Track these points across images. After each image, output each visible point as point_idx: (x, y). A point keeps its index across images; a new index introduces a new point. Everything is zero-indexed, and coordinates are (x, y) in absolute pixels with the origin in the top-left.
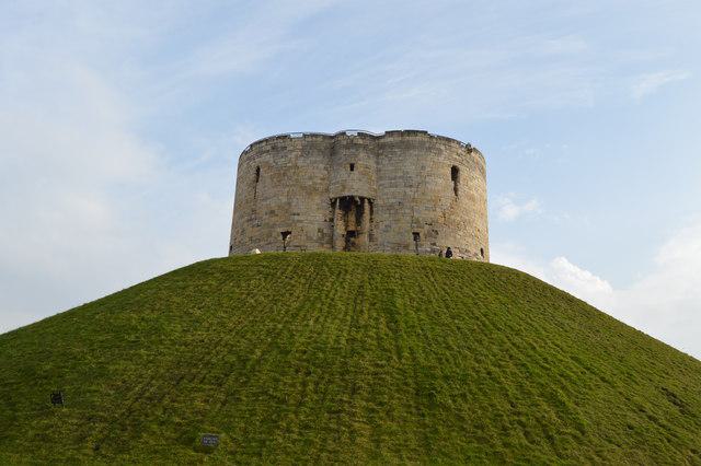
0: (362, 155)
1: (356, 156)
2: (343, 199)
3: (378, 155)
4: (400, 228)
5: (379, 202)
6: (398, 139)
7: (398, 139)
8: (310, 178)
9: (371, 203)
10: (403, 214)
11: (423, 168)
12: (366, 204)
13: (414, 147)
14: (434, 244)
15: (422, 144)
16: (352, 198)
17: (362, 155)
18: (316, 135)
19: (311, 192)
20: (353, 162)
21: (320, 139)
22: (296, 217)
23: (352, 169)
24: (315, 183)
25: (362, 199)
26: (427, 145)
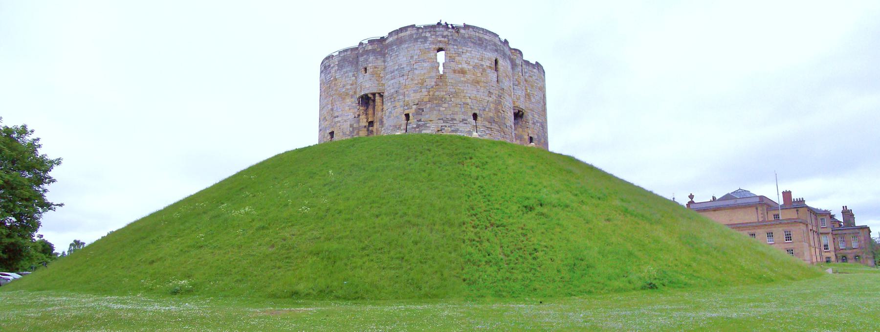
0: (371, 58)
1: (367, 60)
2: (362, 97)
3: (384, 55)
5: (386, 94)
9: (381, 96)
11: (412, 57)
12: (377, 98)
13: (405, 41)
14: (420, 120)
15: (411, 36)
16: (366, 95)
18: (346, 51)
19: (343, 97)
21: (349, 53)
22: (337, 119)
25: (374, 94)
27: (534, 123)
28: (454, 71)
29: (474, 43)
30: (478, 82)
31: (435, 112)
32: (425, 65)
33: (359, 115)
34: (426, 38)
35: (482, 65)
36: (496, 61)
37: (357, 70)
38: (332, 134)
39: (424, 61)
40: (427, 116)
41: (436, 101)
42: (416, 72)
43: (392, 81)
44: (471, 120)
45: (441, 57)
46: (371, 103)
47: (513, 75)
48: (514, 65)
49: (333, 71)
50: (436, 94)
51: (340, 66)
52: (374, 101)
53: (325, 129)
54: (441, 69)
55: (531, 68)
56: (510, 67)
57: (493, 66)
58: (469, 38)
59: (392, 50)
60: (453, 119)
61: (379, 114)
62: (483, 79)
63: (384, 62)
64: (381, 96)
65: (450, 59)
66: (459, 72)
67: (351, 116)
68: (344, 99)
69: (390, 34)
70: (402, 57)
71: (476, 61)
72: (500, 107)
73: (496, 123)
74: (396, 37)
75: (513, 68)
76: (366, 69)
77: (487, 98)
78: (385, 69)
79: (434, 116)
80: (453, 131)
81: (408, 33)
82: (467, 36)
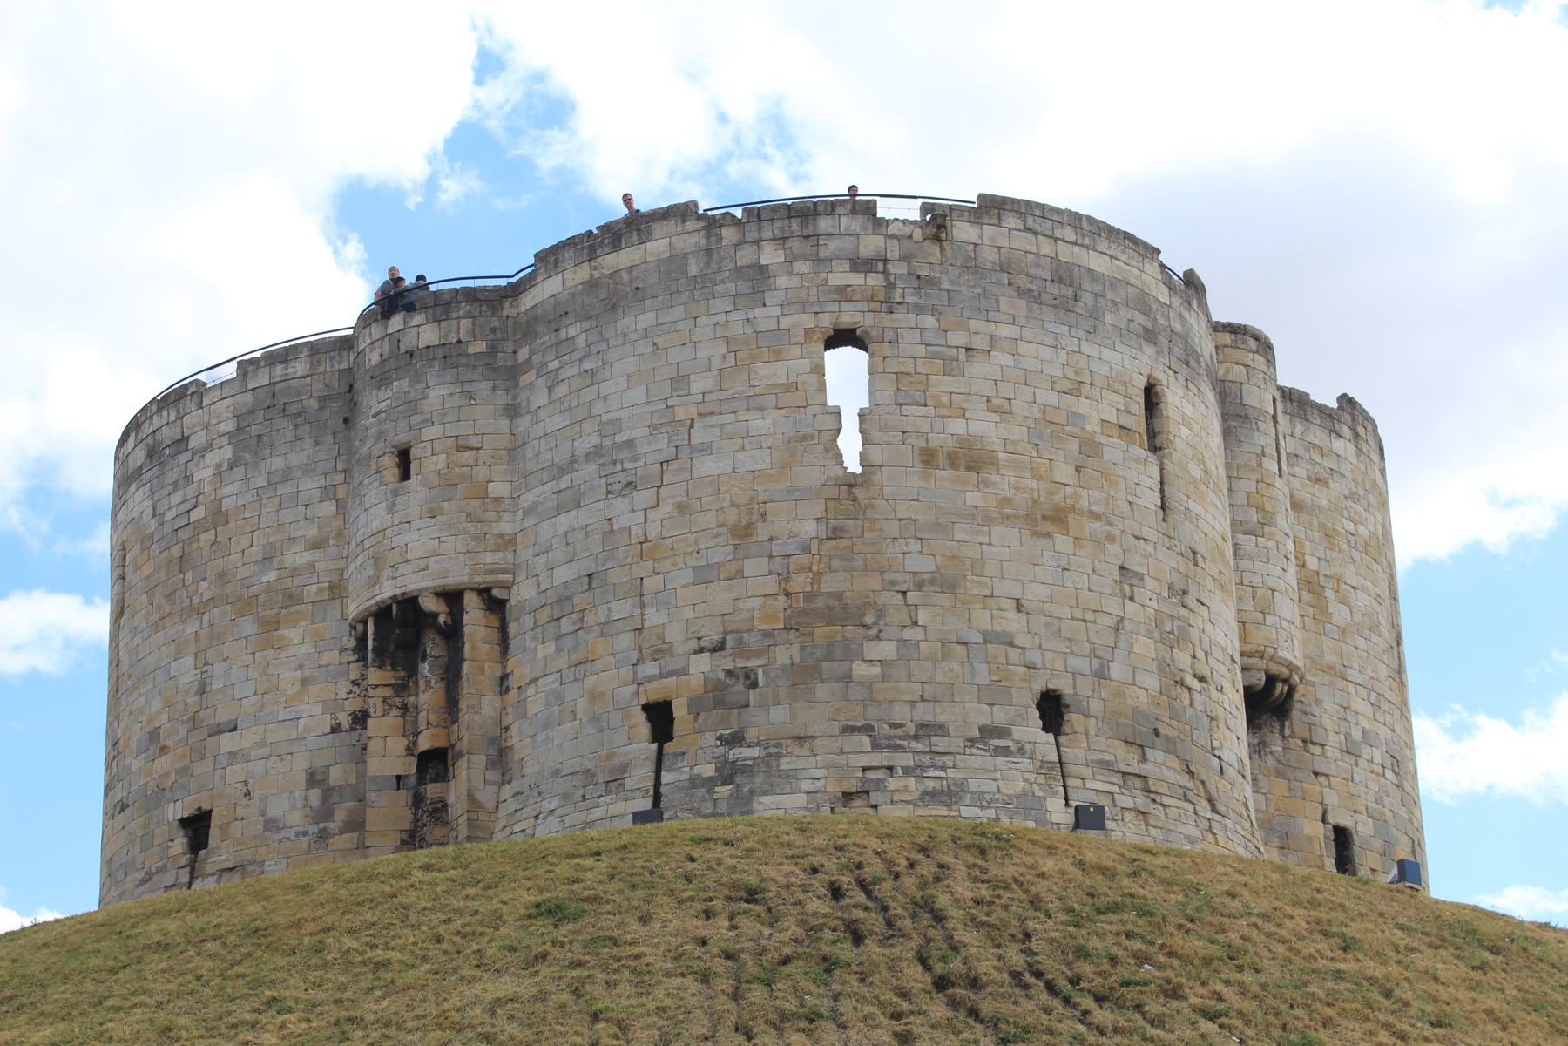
0: (438, 392)
1: (412, 407)
2: (382, 614)
3: (513, 374)
4: (595, 696)
5: (523, 593)
6: (577, 274)
7: (577, 274)
8: (267, 560)
9: (496, 606)
10: (607, 628)
11: (680, 382)
12: (475, 617)
14: (736, 740)
15: (673, 264)
16: (409, 603)
17: (437, 393)
18: (279, 356)
19: (273, 612)
20: (403, 437)
21: (298, 367)
22: (227, 742)
23: (406, 476)
24: (294, 572)
25: (453, 598)
26: (693, 269)
27: (1350, 750)
28: (928, 458)
29: (1032, 297)
30: (1059, 518)
31: (822, 691)
32: (760, 424)
33: (360, 719)
34: (760, 273)
35: (1076, 418)
36: (1151, 397)
37: (349, 463)
38: (197, 827)
39: (752, 402)
40: (779, 714)
41: (824, 625)
42: (707, 466)
43: (564, 521)
44: (1031, 730)
45: (847, 376)
46: (433, 646)
47: (1234, 471)
48: (1235, 416)
49: (203, 473)
50: (830, 584)
51: (247, 441)
52: (453, 634)
53: (155, 798)
54: (850, 445)
55: (1318, 435)
56: (1216, 427)
57: (1137, 421)
58: (1004, 267)
59: (562, 346)
60: (926, 730)
61: (480, 707)
62: (1089, 498)
63: (512, 412)
64: (496, 606)
65: (895, 388)
66: (953, 461)
67: (314, 716)
68: (270, 626)
69: (549, 259)
70: (619, 384)
71: (1047, 397)
72: (1183, 658)
73: (1171, 747)
74: (583, 273)
75: (1227, 433)
76: (404, 458)
77: (1113, 605)
78: (514, 450)
79: (820, 711)
80: (929, 796)
81: (658, 246)
82: (989, 256)
